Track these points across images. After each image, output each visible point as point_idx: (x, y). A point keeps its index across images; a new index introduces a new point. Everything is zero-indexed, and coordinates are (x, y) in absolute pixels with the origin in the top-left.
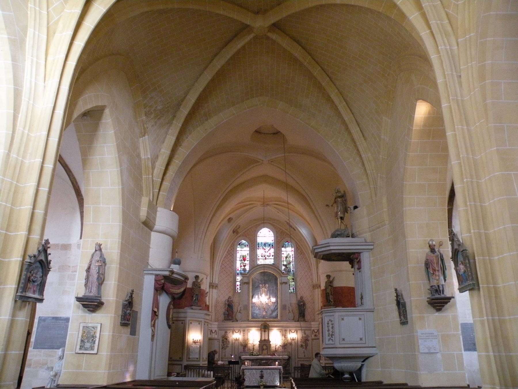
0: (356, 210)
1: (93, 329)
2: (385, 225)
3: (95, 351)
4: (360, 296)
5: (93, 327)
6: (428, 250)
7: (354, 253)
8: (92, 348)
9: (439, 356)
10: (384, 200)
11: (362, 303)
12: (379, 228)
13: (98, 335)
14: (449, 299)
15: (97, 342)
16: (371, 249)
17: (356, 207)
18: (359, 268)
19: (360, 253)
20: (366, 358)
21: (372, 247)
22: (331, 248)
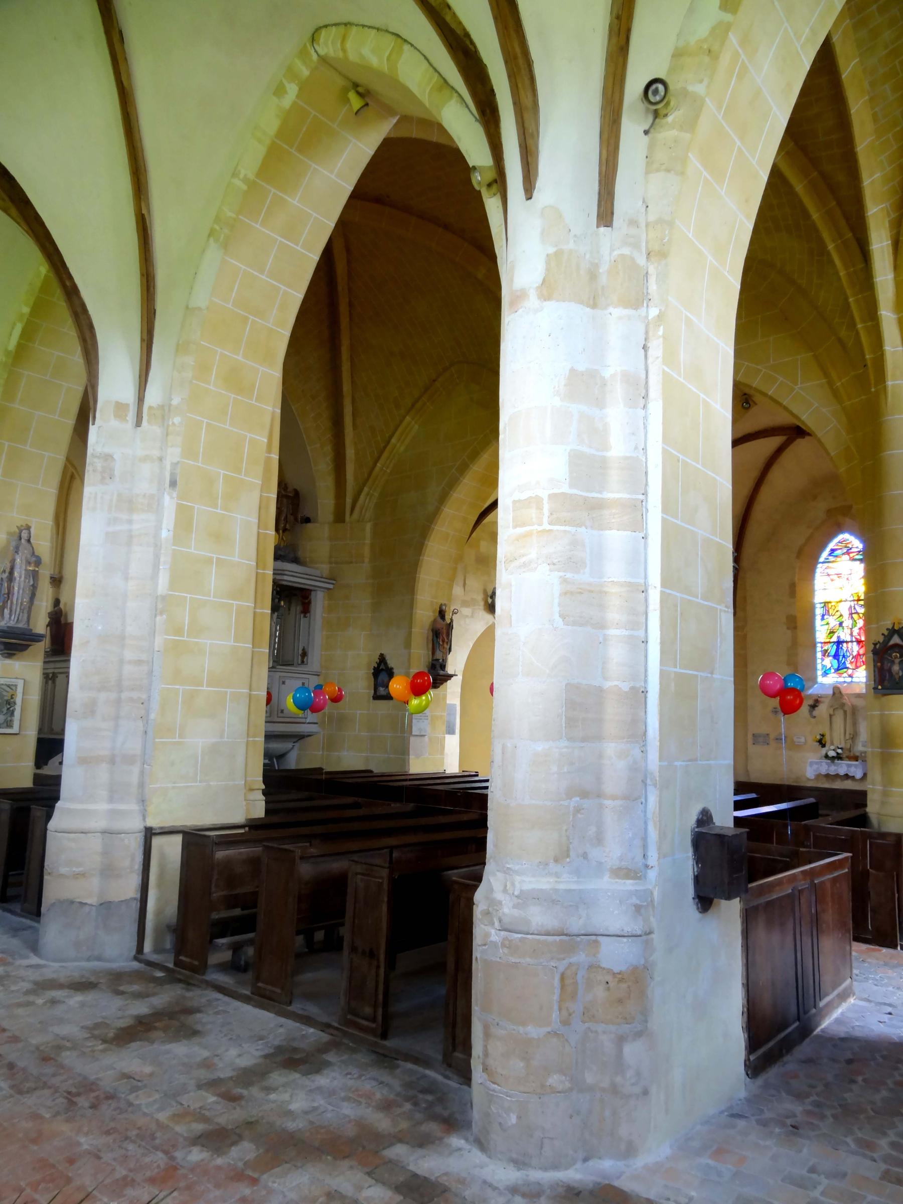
0: (309, 525)
1: (8, 689)
2: (363, 562)
3: (15, 729)
4: (300, 652)
5: (9, 686)
6: (437, 614)
7: (302, 590)
8: (9, 724)
9: (426, 738)
10: (368, 527)
11: (303, 662)
12: (351, 562)
13: (18, 699)
14: (450, 677)
15: (17, 713)
16: (329, 589)
17: (308, 520)
18: (306, 610)
19: (311, 590)
20: (300, 737)
21: (331, 586)
22: (286, 578)
